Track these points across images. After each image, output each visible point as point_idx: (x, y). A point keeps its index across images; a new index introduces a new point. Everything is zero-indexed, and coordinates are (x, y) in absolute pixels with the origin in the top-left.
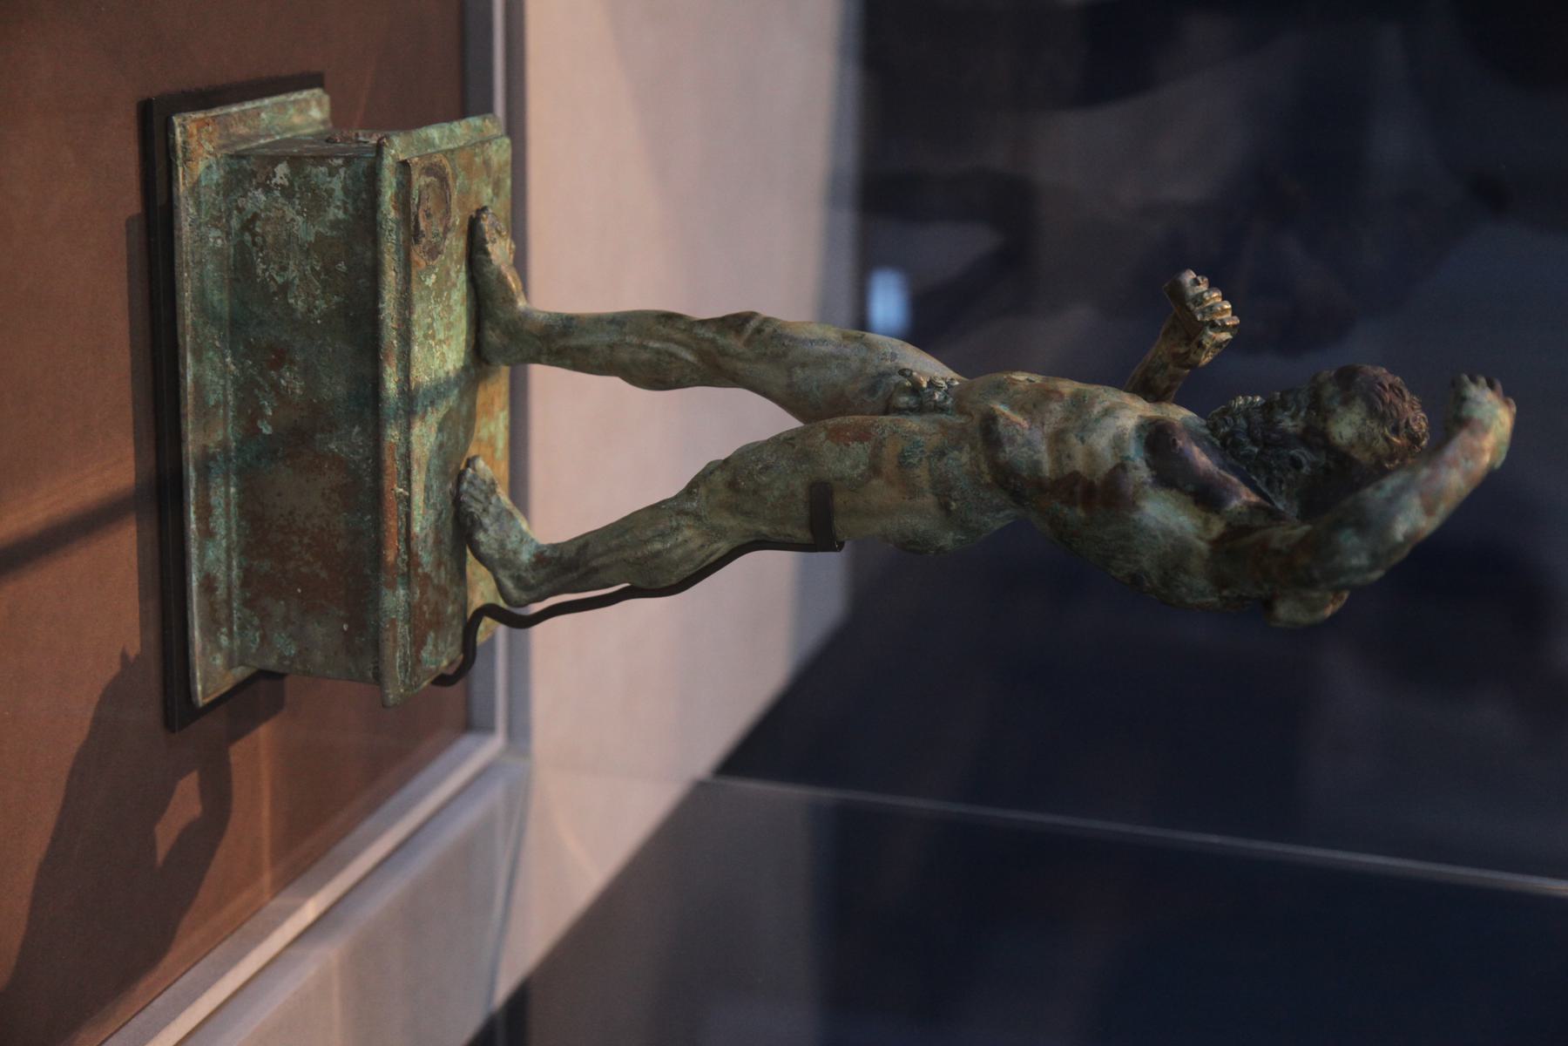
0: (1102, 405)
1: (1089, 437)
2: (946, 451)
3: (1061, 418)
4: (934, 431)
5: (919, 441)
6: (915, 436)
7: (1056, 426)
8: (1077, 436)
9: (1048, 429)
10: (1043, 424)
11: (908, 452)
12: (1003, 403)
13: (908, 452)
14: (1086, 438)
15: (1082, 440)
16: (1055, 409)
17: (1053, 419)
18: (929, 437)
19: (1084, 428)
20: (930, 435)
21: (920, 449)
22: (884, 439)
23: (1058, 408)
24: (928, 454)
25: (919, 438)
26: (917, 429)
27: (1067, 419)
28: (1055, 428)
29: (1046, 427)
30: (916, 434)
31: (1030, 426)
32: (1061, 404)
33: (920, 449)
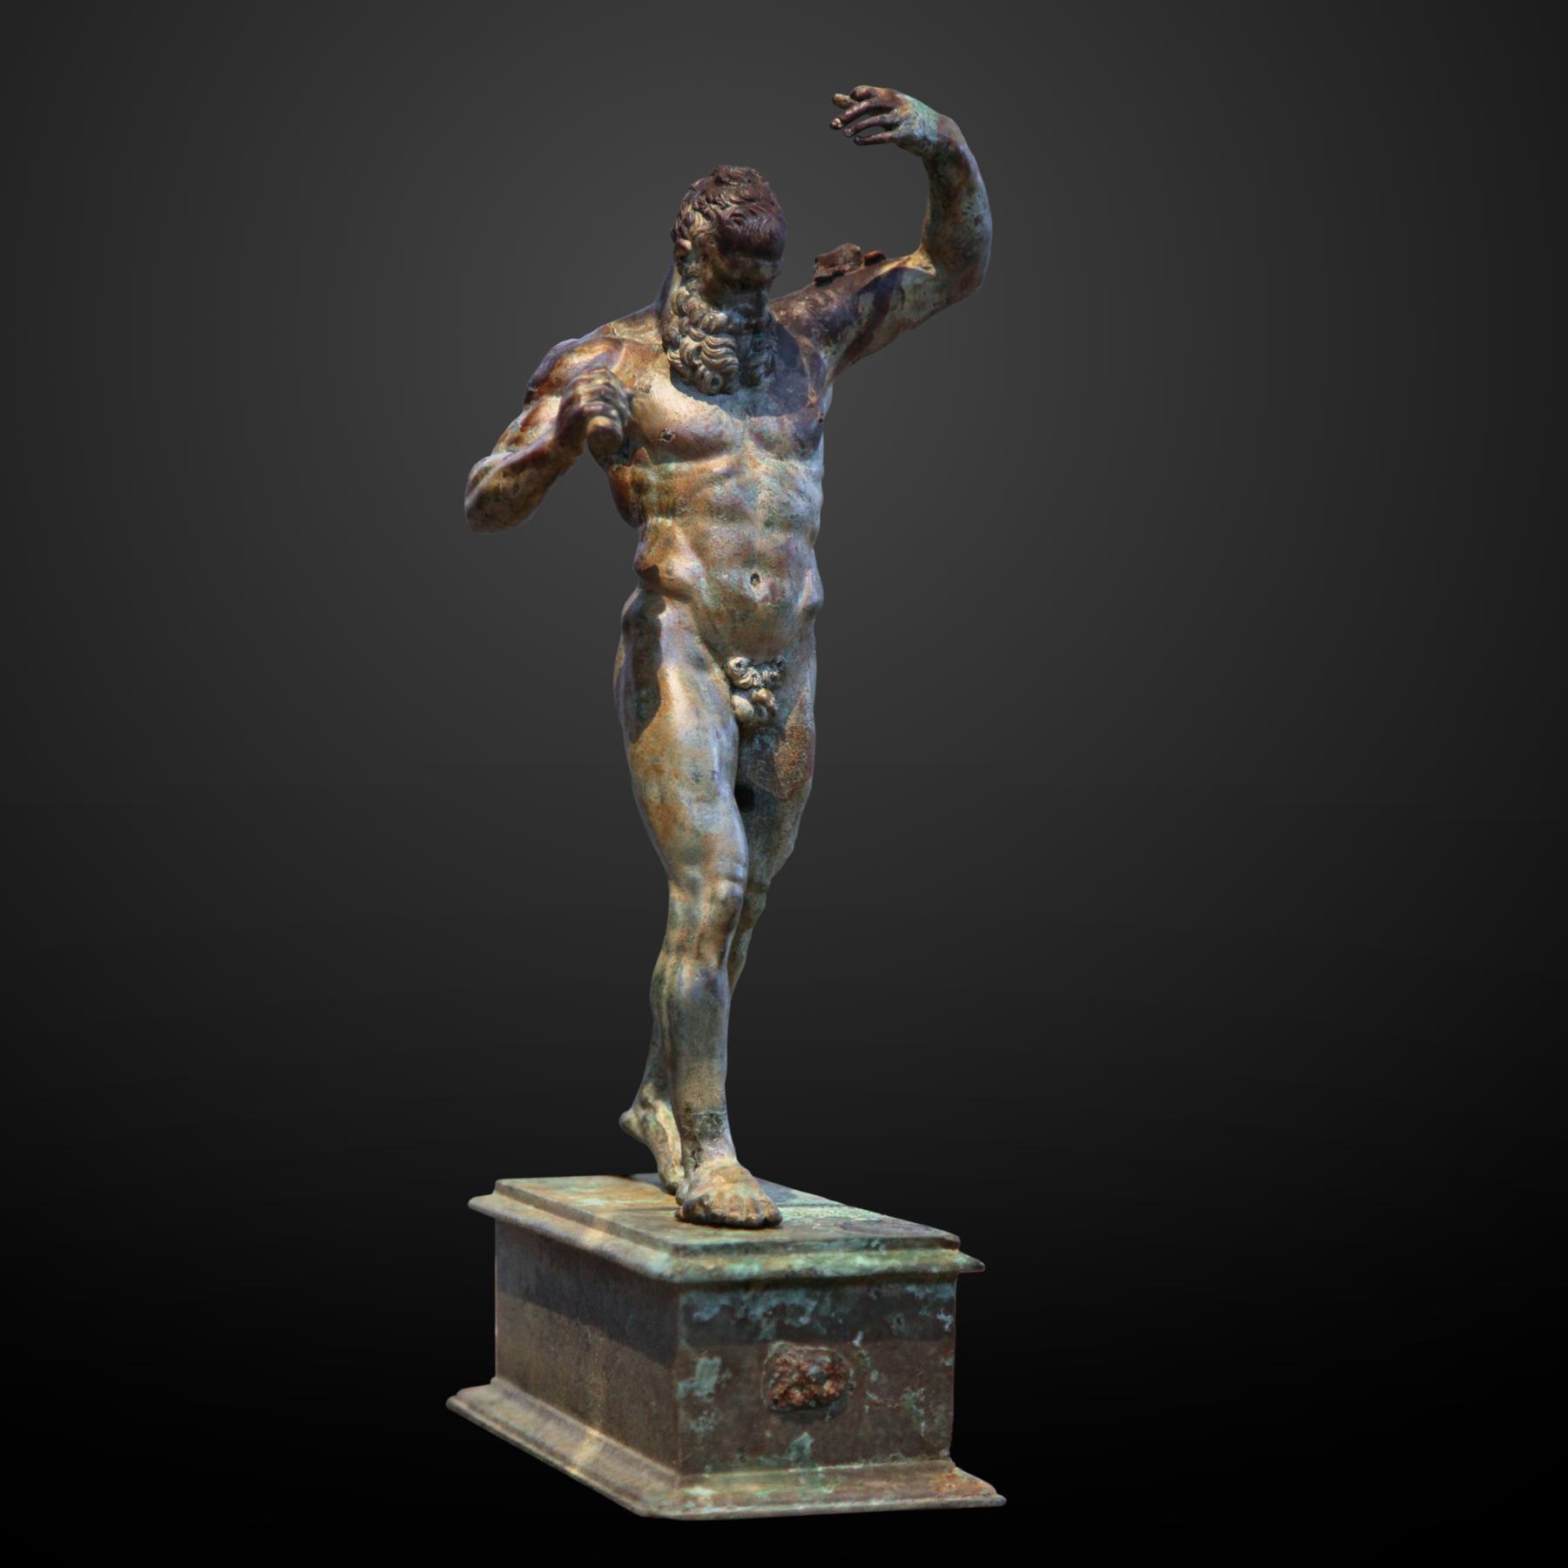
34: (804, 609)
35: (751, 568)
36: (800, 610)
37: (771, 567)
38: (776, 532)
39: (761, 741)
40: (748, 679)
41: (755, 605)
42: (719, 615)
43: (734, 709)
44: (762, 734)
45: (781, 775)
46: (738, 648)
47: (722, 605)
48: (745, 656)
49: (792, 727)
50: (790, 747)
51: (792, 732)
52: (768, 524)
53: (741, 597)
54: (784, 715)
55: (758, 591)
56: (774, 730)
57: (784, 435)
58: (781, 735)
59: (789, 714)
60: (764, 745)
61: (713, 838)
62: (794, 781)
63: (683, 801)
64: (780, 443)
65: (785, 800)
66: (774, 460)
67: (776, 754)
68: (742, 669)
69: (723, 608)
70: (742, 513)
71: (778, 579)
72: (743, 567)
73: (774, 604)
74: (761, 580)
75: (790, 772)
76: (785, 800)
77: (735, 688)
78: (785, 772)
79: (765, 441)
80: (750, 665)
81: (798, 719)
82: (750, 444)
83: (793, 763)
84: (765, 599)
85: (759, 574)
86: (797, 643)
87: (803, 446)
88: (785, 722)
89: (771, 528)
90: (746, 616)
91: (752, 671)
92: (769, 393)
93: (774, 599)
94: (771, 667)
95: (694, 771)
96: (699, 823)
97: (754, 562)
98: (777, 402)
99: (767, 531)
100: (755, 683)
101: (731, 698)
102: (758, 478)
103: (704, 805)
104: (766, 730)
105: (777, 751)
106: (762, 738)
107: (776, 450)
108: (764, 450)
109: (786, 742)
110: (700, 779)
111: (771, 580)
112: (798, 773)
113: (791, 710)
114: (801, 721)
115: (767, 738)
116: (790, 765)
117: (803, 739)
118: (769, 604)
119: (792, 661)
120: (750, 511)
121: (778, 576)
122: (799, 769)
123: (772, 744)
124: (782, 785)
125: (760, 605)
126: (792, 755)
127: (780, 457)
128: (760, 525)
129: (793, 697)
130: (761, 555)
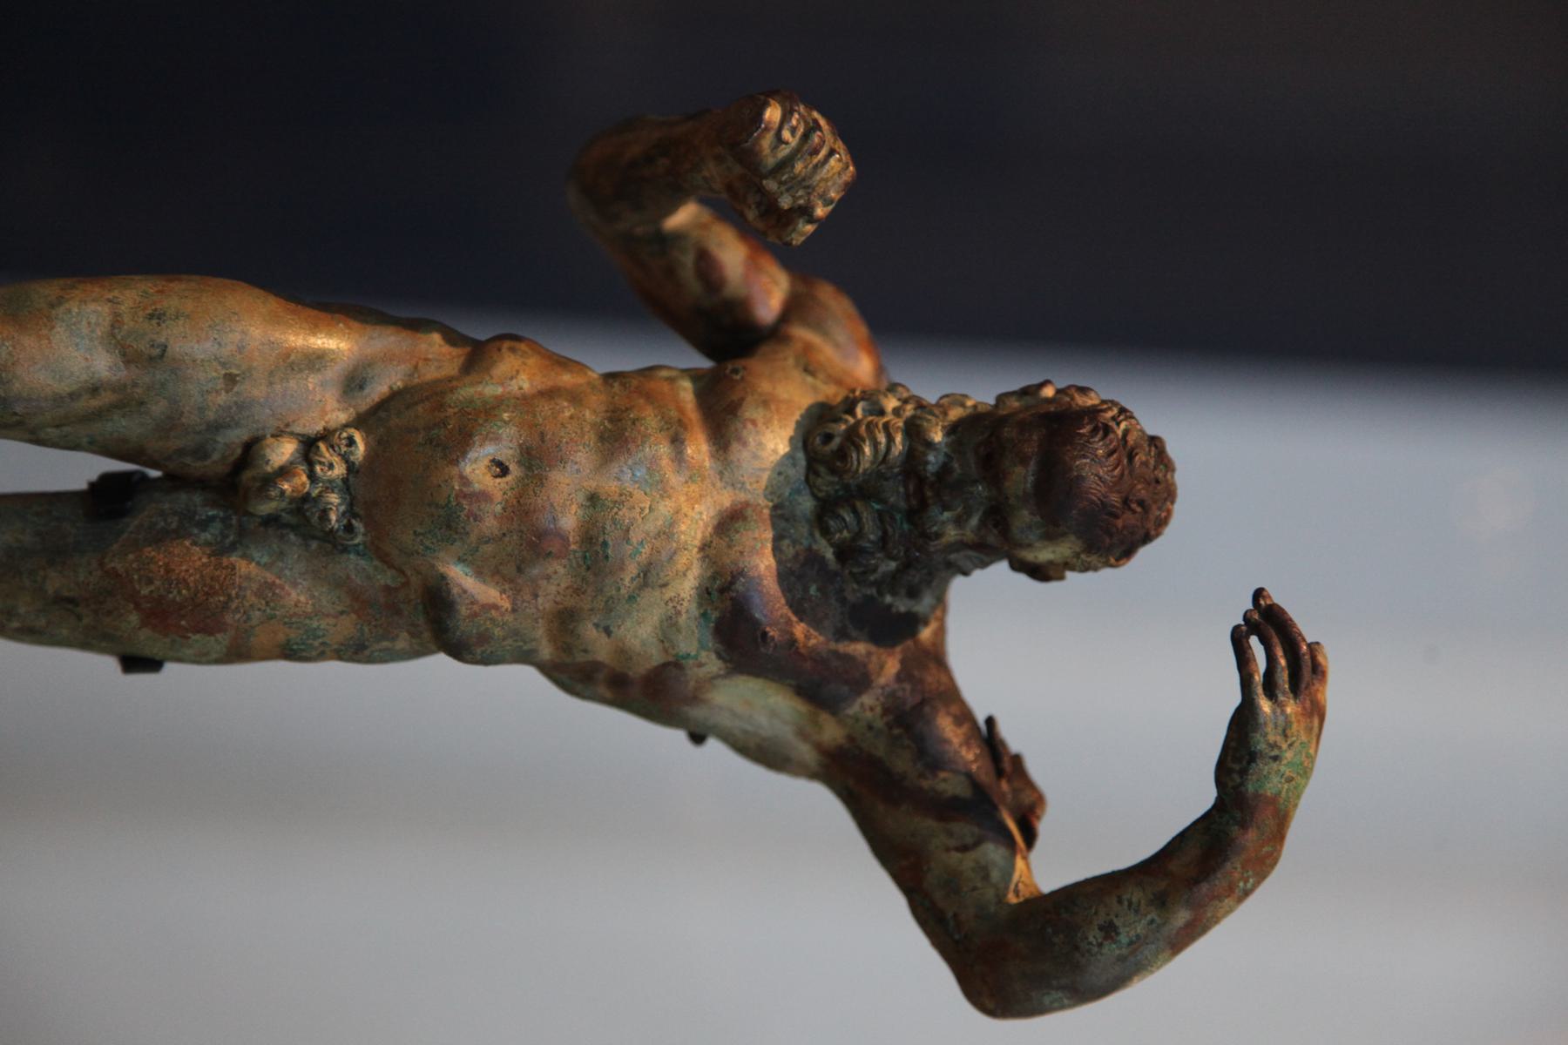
0: (638, 558)
1: (619, 627)
2: (366, 643)
3: (567, 588)
4: (340, 608)
5: (315, 629)
6: (307, 621)
7: (558, 599)
8: (597, 626)
9: (545, 603)
10: (536, 596)
11: (297, 644)
12: (461, 560)
13: (297, 644)
14: (614, 629)
15: (608, 631)
16: (556, 572)
17: (553, 589)
18: (332, 621)
19: (609, 610)
20: (336, 617)
21: (320, 640)
22: (252, 627)
23: (562, 571)
24: (336, 646)
25: (315, 624)
26: (309, 609)
27: (578, 591)
28: (556, 603)
29: (540, 600)
30: (311, 619)
31: (514, 603)
32: (564, 561)
33: (320, 640)
34: (443, 577)
35: (519, 462)
36: (442, 569)
37: (519, 497)
38: (580, 512)
39: (212, 519)
40: (327, 455)
41: (455, 462)
42: (441, 406)
43: (273, 436)
44: (225, 521)
45: (149, 552)
46: (379, 442)
47: (456, 410)
48: (367, 457)
49: (234, 568)
50: (198, 563)
51: (227, 567)
52: (593, 499)
53: (471, 436)
54: (256, 555)
55: (476, 467)
56: (232, 538)
57: (741, 553)
58: (220, 550)
59: (258, 563)
60: (204, 525)
61: (44, 332)
62: (136, 577)
63: (116, 293)
64: (729, 547)
65: (101, 565)
66: (699, 536)
67: (187, 543)
68: (344, 449)
69: (450, 411)
70: (612, 454)
71: (498, 508)
72: (520, 446)
73: (457, 496)
74: (498, 480)
75: (152, 566)
76: (101, 565)
77: (309, 446)
78: (152, 558)
79: (730, 522)
80: (351, 467)
81: (248, 578)
82: (726, 499)
83: (168, 571)
84: (465, 481)
85: (509, 478)
86: (382, 582)
87: (722, 591)
88: (244, 556)
89: (588, 504)
90: (438, 445)
91: (339, 470)
92: (809, 549)
93: (465, 496)
94: (344, 514)
95: (168, 314)
96: (76, 310)
97: (530, 468)
98: (797, 555)
99: (581, 498)
100: (318, 468)
101: (292, 434)
102: (669, 497)
103: (107, 323)
104: (231, 525)
105: (195, 543)
106: (218, 520)
107: (716, 541)
108: (715, 522)
109: (209, 556)
110: (154, 322)
111: (498, 496)
112: (150, 581)
113: (267, 567)
114: (245, 584)
115: (216, 528)
116: (166, 565)
117: (211, 587)
118: (457, 487)
119: (351, 567)
120: (614, 468)
121: (504, 509)
122: (158, 583)
123: (206, 536)
124: (131, 557)
125: (454, 471)
126: (184, 568)
127: (704, 547)
128: (592, 484)
129: (287, 572)
130: (541, 481)
